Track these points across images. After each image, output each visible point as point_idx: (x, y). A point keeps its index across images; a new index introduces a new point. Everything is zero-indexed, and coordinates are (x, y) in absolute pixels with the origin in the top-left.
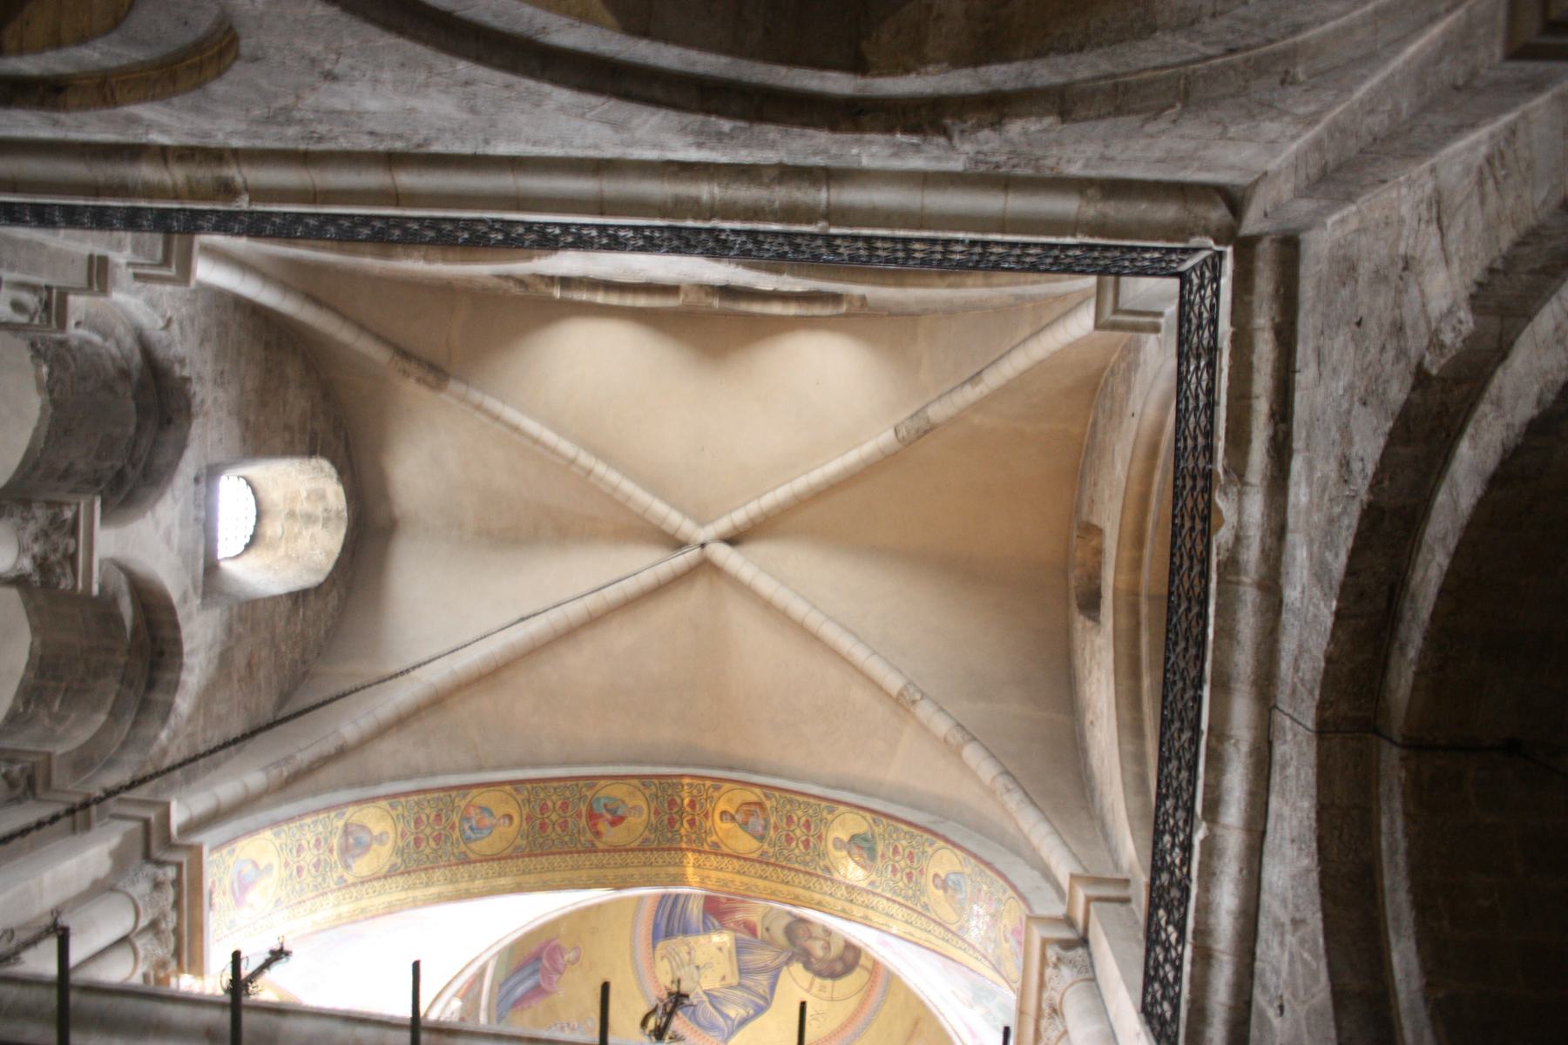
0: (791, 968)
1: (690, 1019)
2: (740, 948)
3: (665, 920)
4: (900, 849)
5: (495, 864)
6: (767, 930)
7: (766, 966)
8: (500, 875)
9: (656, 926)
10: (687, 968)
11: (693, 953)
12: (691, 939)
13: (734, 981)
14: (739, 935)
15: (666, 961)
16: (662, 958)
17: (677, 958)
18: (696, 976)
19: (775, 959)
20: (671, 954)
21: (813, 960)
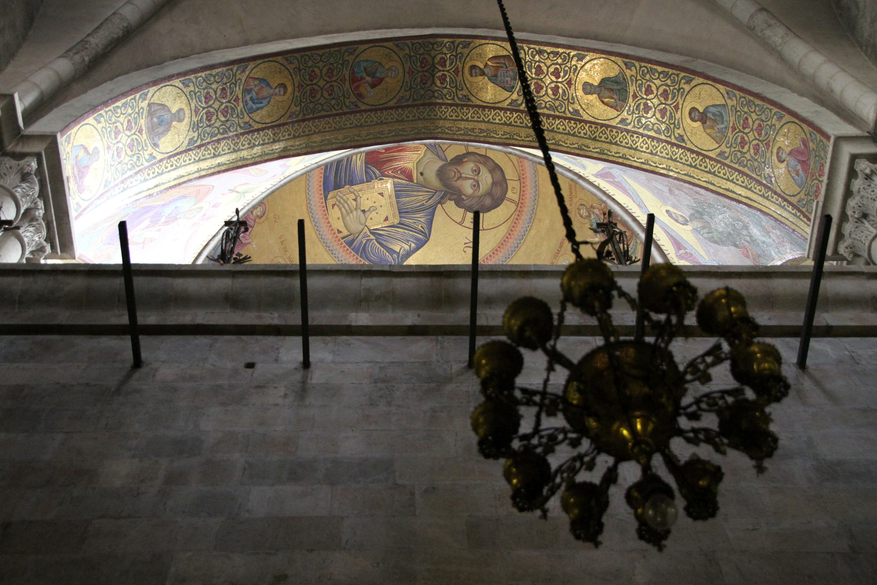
0: (443, 205)
1: (360, 257)
2: (399, 193)
3: (333, 174)
4: (654, 88)
5: (270, 132)
6: (422, 174)
7: (423, 205)
8: (274, 141)
9: (326, 179)
10: (355, 212)
11: (359, 198)
12: (356, 187)
13: (396, 221)
14: (396, 180)
15: (336, 207)
16: (333, 206)
17: (346, 205)
18: (363, 220)
19: (430, 199)
20: (339, 202)
21: (463, 197)
